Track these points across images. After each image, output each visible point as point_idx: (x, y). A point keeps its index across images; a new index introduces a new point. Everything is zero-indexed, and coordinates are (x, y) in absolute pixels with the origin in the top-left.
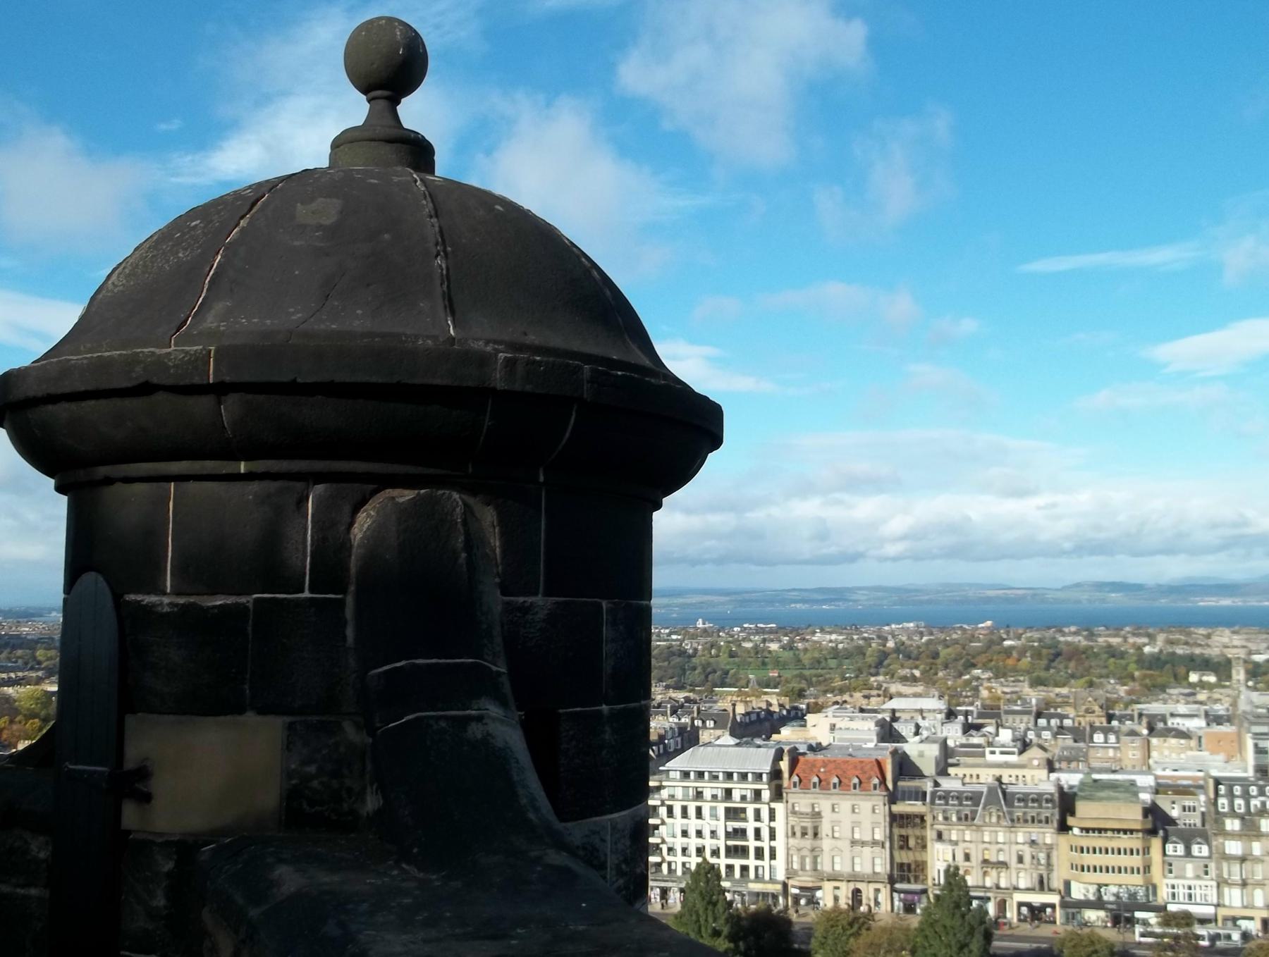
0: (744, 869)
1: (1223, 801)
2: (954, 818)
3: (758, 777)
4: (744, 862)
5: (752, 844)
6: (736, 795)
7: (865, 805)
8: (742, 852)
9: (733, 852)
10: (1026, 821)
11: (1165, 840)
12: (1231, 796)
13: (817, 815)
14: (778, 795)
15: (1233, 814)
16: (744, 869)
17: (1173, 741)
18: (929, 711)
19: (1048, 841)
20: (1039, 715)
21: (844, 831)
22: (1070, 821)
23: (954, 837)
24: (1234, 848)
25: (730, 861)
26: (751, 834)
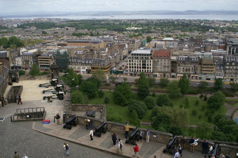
0: (145, 70)
1: (227, 60)
2: (181, 62)
3: (148, 55)
4: (145, 69)
5: (147, 66)
6: (144, 58)
7: (167, 60)
8: (145, 68)
9: (143, 68)
13: (158, 61)
14: (151, 58)
16: (145, 70)
18: (172, 40)
19: (197, 66)
20: (190, 41)
21: (163, 64)
24: (227, 67)
25: (143, 69)
26: (147, 65)
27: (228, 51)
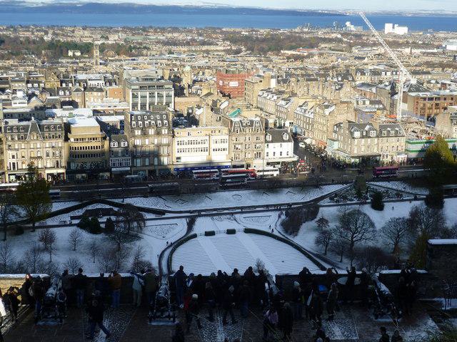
1: (134, 122)
2: (16, 139)
10: (50, 138)
11: (110, 140)
12: (137, 120)
15: (138, 126)
17: (95, 93)
19: (60, 145)
22: (69, 135)
23: (16, 147)
27: (131, 102)
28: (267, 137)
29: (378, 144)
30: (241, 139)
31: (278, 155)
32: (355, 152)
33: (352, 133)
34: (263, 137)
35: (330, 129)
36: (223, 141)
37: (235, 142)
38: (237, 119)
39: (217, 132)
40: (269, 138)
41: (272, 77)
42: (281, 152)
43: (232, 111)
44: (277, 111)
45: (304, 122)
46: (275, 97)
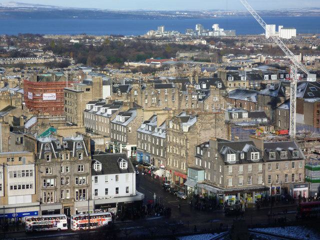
28: (95, 166)
29: (263, 172)
30: (53, 170)
31: (112, 193)
32: (230, 184)
33: (223, 157)
34: (88, 165)
35: (191, 153)
36: (26, 174)
37: (44, 174)
38: (47, 140)
39: (16, 159)
40: (98, 167)
41: (105, 83)
42: (117, 189)
43: (42, 131)
44: (113, 131)
45: (152, 145)
46: (109, 111)
